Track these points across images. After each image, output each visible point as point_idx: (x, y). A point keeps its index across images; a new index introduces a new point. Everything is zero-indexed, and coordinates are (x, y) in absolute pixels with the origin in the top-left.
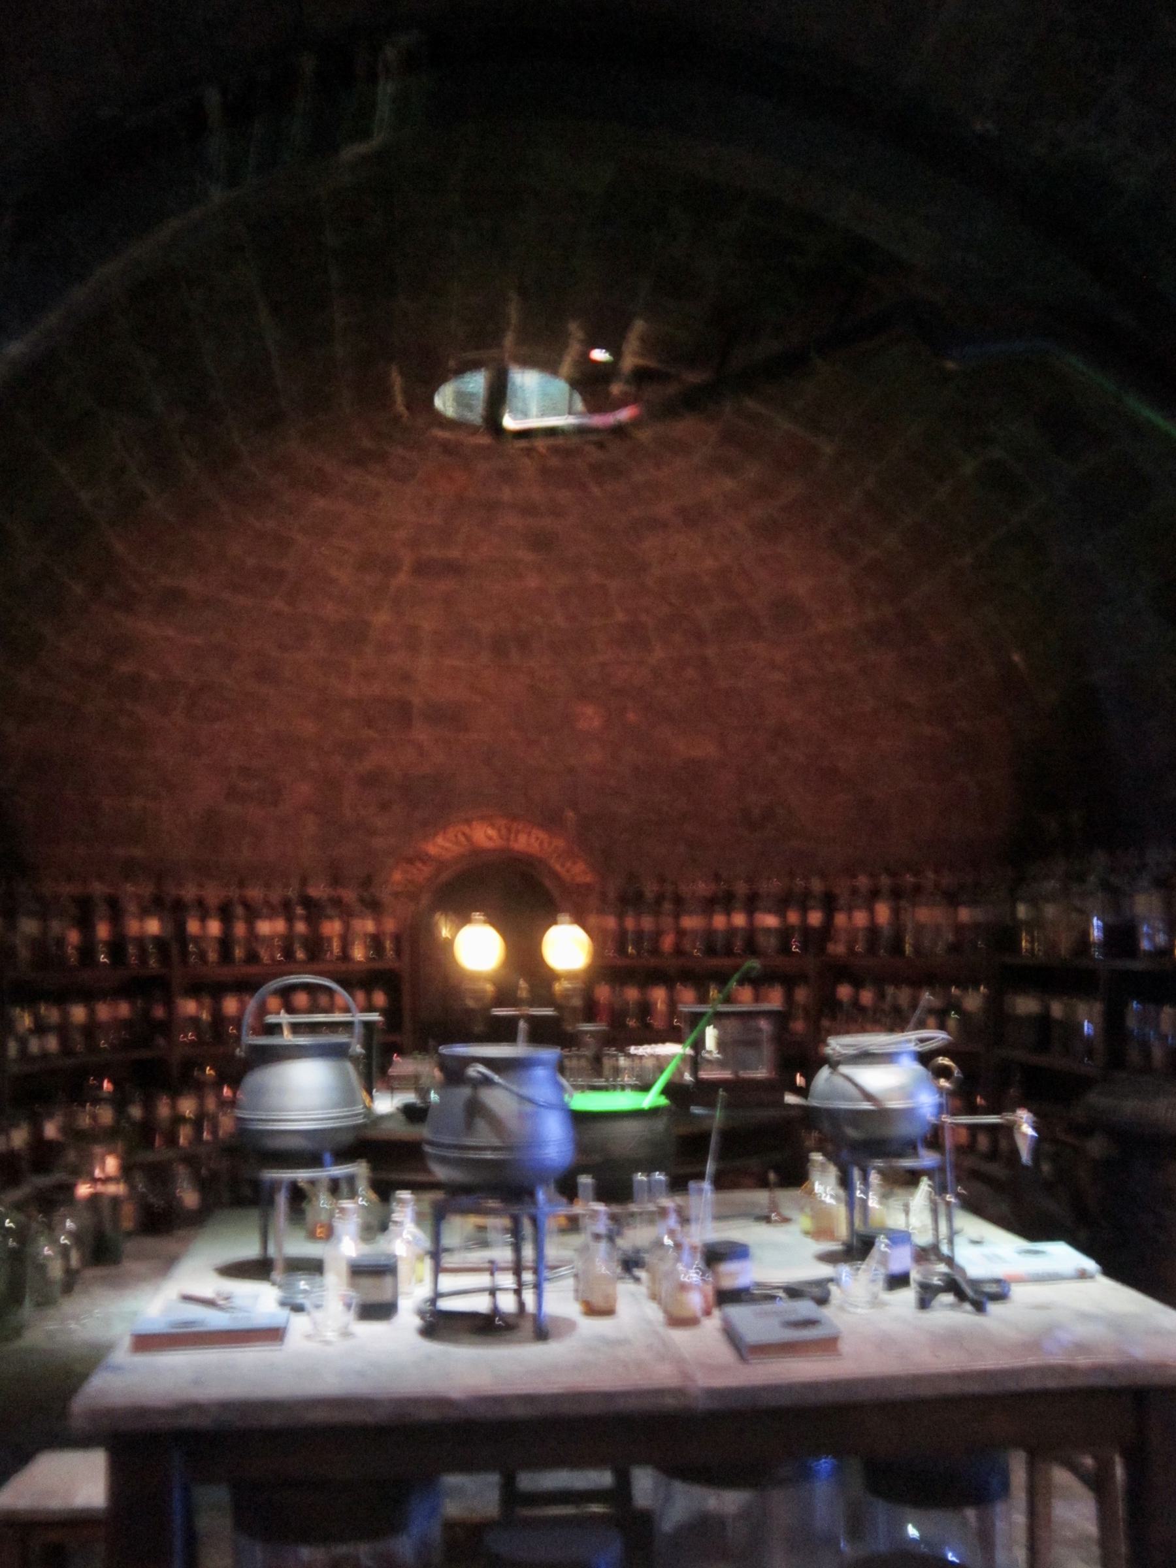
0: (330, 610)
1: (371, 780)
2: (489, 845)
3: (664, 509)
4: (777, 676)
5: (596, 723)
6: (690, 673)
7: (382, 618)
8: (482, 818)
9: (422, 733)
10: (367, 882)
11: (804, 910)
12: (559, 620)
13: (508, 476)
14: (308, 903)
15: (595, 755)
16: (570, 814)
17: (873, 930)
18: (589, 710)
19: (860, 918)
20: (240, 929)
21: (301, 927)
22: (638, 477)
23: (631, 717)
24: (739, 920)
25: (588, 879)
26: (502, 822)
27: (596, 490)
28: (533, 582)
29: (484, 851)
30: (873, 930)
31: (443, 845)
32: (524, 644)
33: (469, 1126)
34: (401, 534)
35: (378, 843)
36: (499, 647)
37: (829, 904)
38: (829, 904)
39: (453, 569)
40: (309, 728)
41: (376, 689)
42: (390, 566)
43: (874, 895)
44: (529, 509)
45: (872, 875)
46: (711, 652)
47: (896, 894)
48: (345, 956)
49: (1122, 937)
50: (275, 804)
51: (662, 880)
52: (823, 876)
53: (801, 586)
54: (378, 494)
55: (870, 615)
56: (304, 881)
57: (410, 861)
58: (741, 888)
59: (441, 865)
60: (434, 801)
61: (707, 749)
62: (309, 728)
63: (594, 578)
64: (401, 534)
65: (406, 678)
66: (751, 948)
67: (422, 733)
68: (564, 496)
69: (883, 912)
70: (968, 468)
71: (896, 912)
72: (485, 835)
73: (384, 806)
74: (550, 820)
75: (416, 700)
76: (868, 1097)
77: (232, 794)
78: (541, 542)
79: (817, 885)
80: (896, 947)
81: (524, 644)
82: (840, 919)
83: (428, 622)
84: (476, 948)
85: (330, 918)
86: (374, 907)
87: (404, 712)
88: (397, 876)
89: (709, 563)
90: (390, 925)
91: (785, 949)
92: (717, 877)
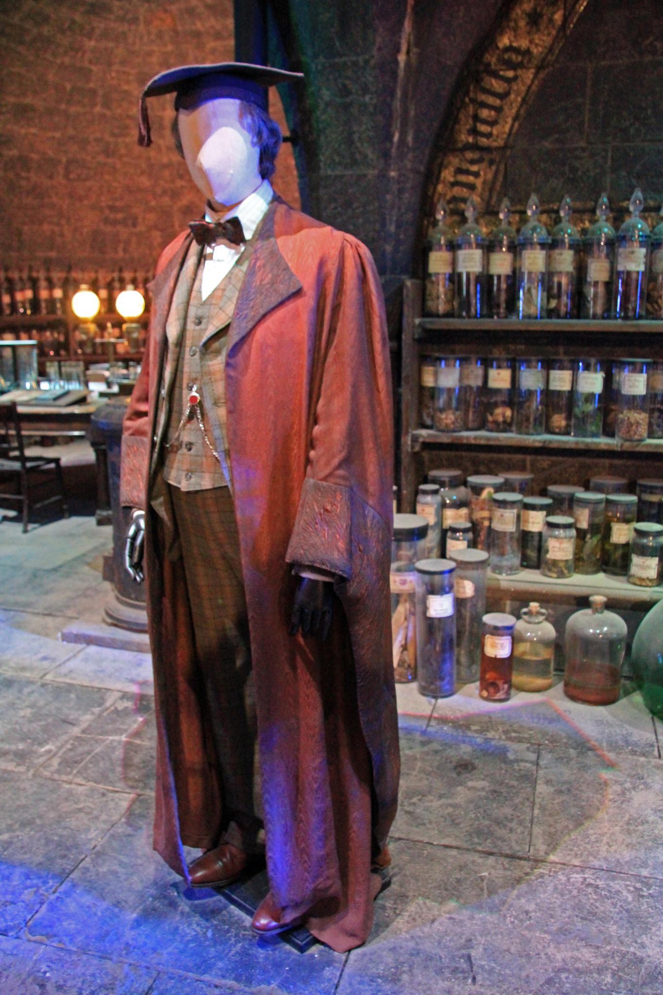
40: (145, 181)
50: (134, 225)
62: (145, 181)
77: (106, 221)
84: (85, 304)
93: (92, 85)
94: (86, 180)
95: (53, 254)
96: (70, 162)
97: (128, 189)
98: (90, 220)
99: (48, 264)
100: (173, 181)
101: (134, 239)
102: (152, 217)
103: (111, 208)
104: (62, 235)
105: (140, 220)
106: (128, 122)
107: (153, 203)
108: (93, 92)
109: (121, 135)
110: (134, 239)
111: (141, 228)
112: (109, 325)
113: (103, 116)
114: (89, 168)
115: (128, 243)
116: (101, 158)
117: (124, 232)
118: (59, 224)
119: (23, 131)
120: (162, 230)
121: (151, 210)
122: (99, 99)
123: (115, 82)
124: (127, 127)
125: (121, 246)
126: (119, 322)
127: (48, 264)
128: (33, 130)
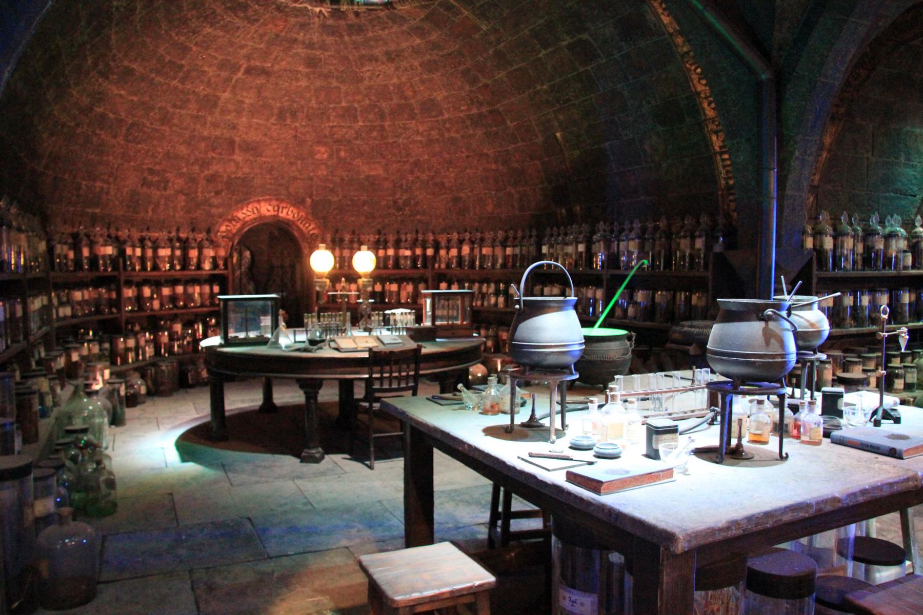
0: (201, 89)
1: (211, 179)
2: (268, 214)
3: (378, 52)
4: (419, 138)
5: (325, 156)
6: (375, 134)
7: (227, 95)
8: (265, 200)
9: (238, 157)
10: (209, 231)
11: (424, 249)
12: (313, 103)
13: (303, 26)
14: (179, 239)
15: (323, 172)
16: (309, 200)
17: (460, 257)
18: (323, 149)
19: (454, 252)
20: (149, 253)
21: (178, 253)
22: (370, 34)
23: (342, 154)
24: (391, 252)
25: (316, 231)
26: (274, 203)
27: (347, 38)
28: (303, 83)
29: (265, 217)
30: (460, 257)
31: (247, 214)
32: (294, 114)
33: (767, 343)
34: (243, 52)
35: (214, 211)
36: (281, 115)
37: (437, 248)
38: (437, 248)
39: (266, 73)
40: (183, 150)
41: (218, 132)
42: (235, 68)
43: (461, 242)
44: (310, 46)
45: (458, 233)
46: (387, 124)
47: (472, 242)
48: (199, 267)
49: (613, 260)
50: (165, 189)
51: (353, 233)
52: (434, 233)
53: (439, 96)
54: (238, 28)
55: (475, 111)
56: (178, 230)
57: (230, 221)
58: (391, 238)
59: (245, 224)
60: (242, 191)
61: (380, 171)
62: (183, 150)
63: (335, 83)
64: (243, 52)
65: (234, 127)
66: (397, 264)
67: (238, 157)
68: (330, 40)
69: (466, 250)
70: (567, 41)
71: (472, 249)
72: (267, 209)
73: (217, 193)
74: (298, 202)
75: (237, 139)
76: (812, 325)
78: (312, 63)
79: (431, 237)
80: (472, 265)
81: (294, 114)
82: (443, 252)
83: (249, 99)
85: (193, 248)
86: (214, 244)
87: (231, 143)
88: (223, 228)
89: (395, 80)
90: (222, 253)
91: (414, 266)
92: (379, 233)
93: (183, 62)
94: (139, 143)
95: (98, 211)
96: (132, 125)
97: (168, 156)
98: (131, 181)
99: (94, 220)
100: (206, 153)
101: (163, 201)
102: (180, 182)
103: (151, 171)
104: (108, 193)
105: (170, 185)
106: (191, 97)
107: (185, 170)
108: (183, 66)
109: (181, 108)
110: (163, 201)
111: (170, 192)
112: (343, 279)
113: (176, 88)
114: (145, 133)
115: (157, 205)
116: (157, 125)
117: (156, 194)
118: (108, 183)
119: (116, 92)
120: (186, 195)
121: (181, 175)
122: (181, 74)
123: (200, 63)
124: (188, 101)
125: (152, 206)
126: (352, 277)
127: (94, 220)
128: (123, 92)
